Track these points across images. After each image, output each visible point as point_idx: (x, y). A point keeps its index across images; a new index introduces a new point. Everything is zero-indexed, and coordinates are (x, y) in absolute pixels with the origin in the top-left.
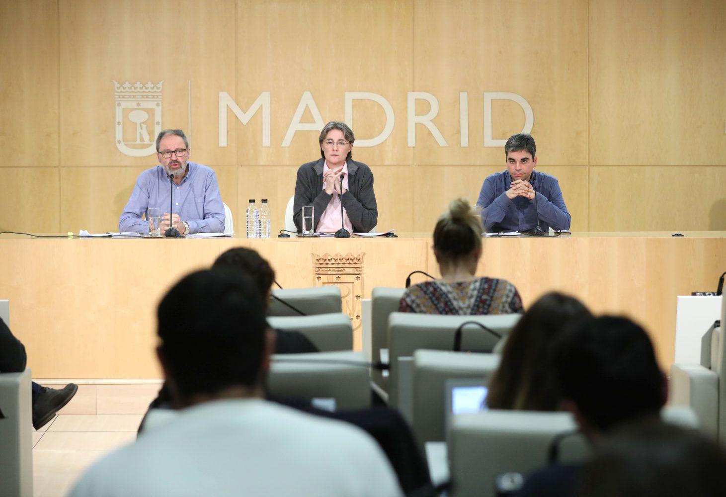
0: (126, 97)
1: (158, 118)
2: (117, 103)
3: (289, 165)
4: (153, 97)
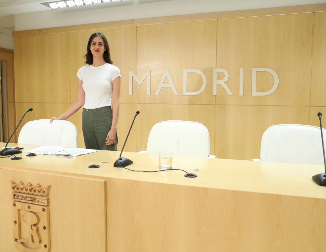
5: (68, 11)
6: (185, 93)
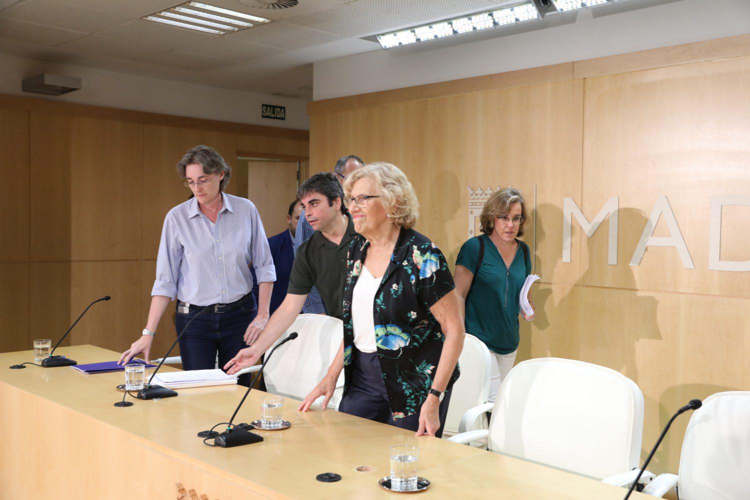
0: (478, 204)
5: (420, 49)
6: (715, 264)
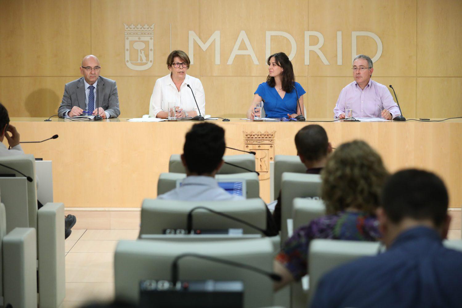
0: (132, 34)
1: (151, 47)
2: (126, 37)
3: (232, 76)
4: (148, 34)
